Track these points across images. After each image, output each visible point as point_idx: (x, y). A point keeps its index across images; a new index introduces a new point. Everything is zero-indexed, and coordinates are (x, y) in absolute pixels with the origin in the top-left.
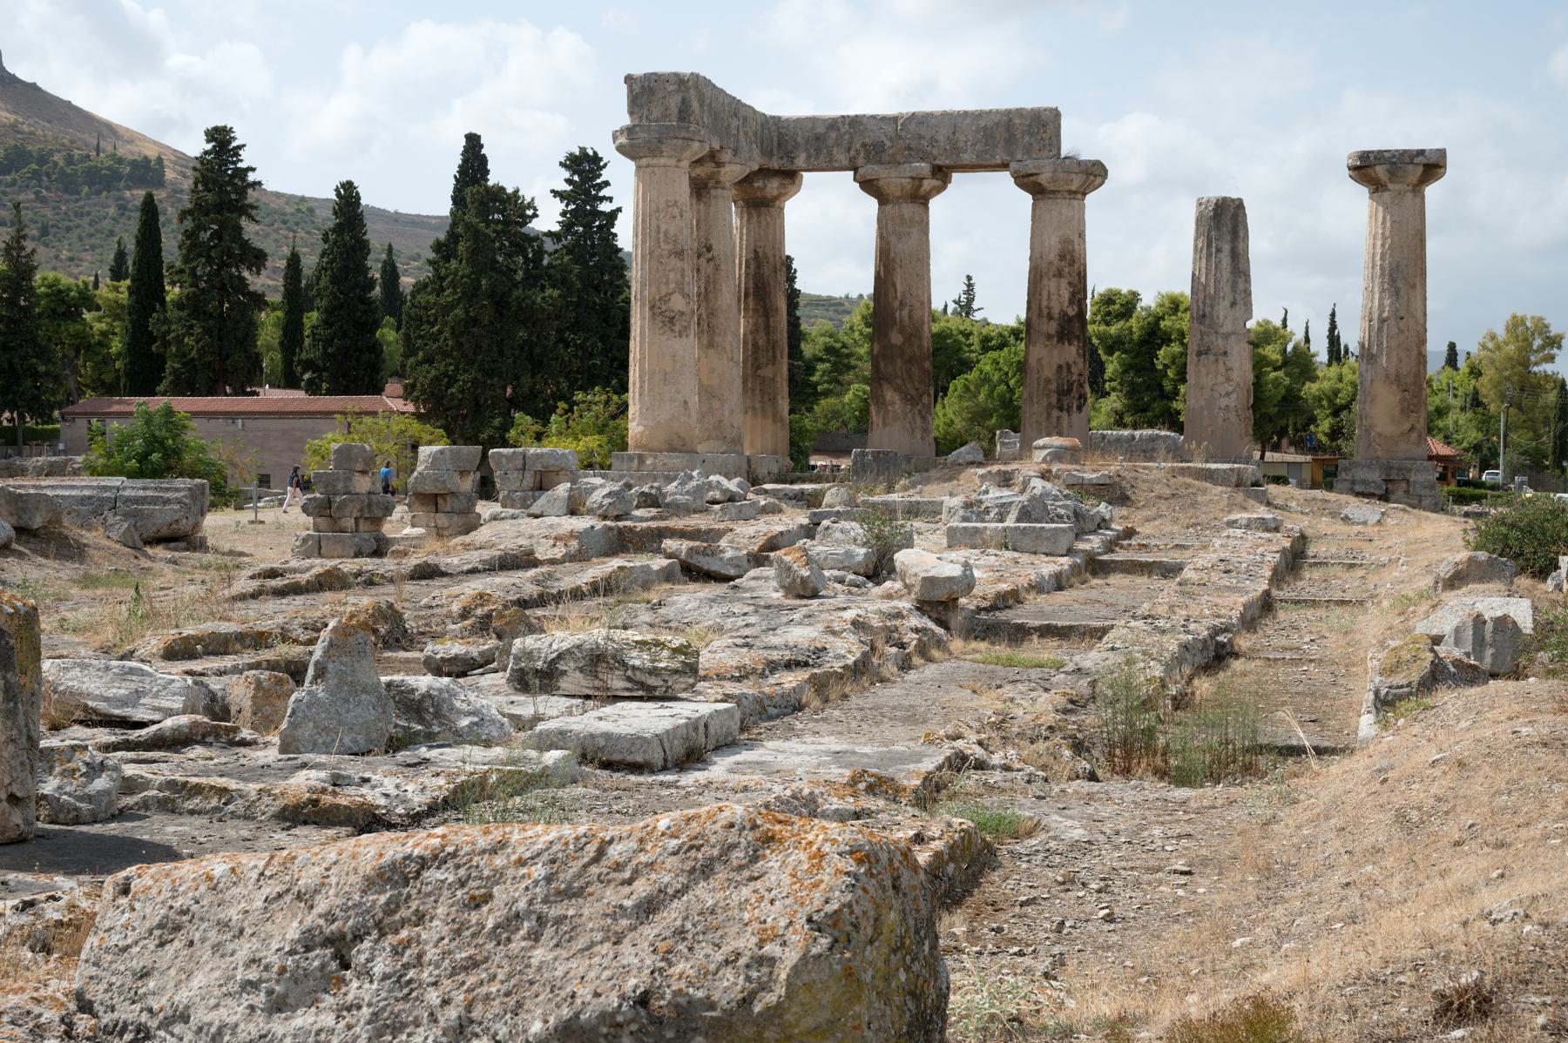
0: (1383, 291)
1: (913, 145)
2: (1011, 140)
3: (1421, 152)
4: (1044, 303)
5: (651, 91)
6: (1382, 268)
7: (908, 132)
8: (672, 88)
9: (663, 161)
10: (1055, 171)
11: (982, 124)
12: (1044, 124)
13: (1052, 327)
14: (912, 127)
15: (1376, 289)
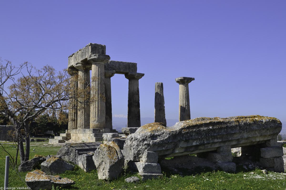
0: (186, 100)
1: (112, 67)
2: (129, 68)
3: (191, 78)
4: (135, 99)
5: (96, 47)
6: (185, 97)
7: (111, 64)
8: (100, 48)
9: (102, 63)
10: (138, 75)
11: (124, 64)
12: (134, 66)
13: (136, 104)
14: (111, 63)
15: (184, 100)
